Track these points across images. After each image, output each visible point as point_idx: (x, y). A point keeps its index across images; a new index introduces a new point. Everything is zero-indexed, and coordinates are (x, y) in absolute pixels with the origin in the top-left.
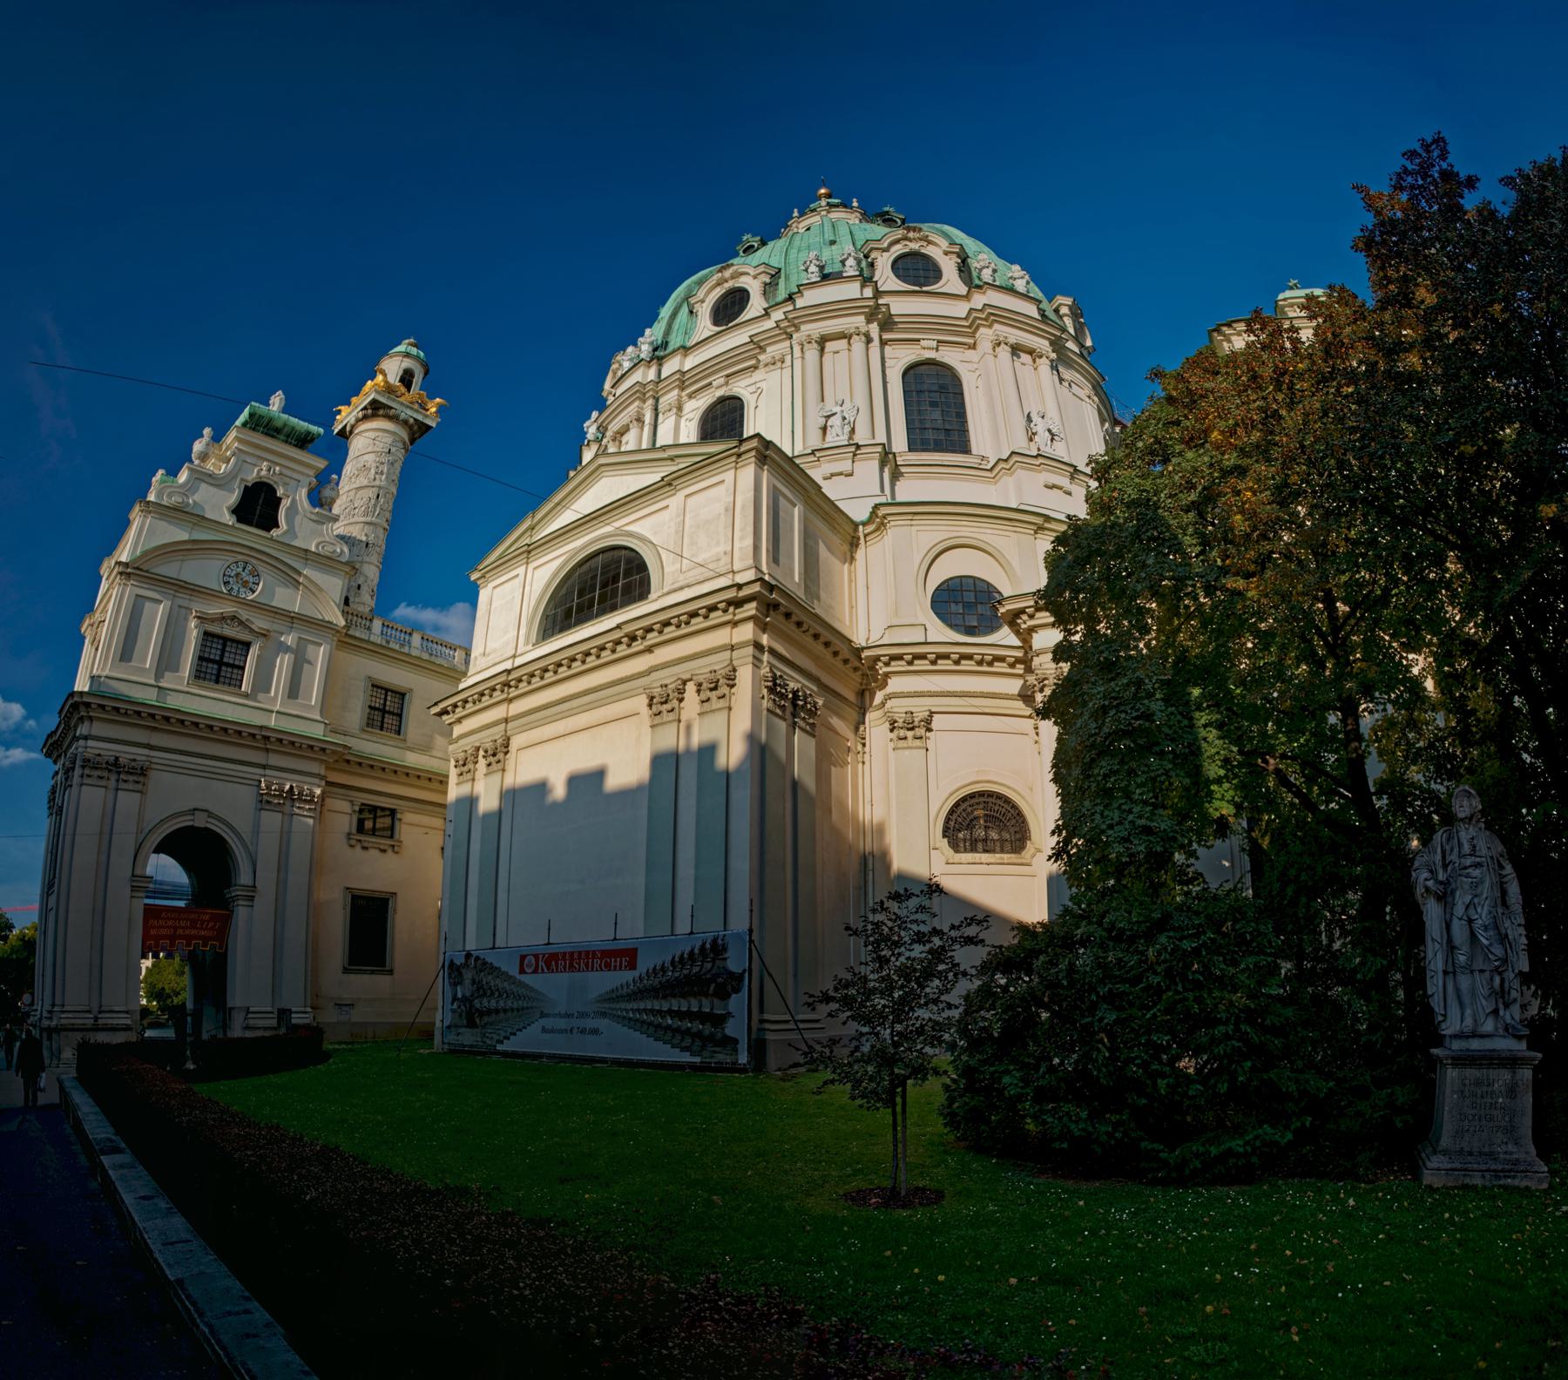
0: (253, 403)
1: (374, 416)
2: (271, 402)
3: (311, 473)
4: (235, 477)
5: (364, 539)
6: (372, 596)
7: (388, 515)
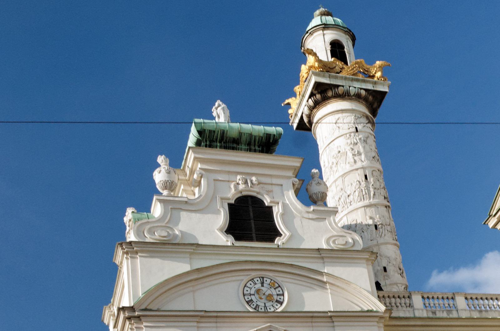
0: (197, 120)
1: (325, 99)
2: (214, 114)
3: (290, 173)
4: (214, 198)
5: (370, 222)
6: (401, 274)
7: (383, 192)
